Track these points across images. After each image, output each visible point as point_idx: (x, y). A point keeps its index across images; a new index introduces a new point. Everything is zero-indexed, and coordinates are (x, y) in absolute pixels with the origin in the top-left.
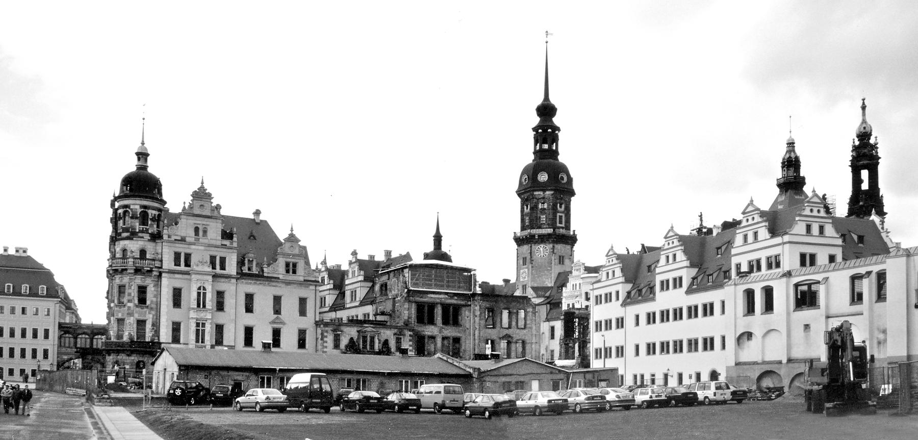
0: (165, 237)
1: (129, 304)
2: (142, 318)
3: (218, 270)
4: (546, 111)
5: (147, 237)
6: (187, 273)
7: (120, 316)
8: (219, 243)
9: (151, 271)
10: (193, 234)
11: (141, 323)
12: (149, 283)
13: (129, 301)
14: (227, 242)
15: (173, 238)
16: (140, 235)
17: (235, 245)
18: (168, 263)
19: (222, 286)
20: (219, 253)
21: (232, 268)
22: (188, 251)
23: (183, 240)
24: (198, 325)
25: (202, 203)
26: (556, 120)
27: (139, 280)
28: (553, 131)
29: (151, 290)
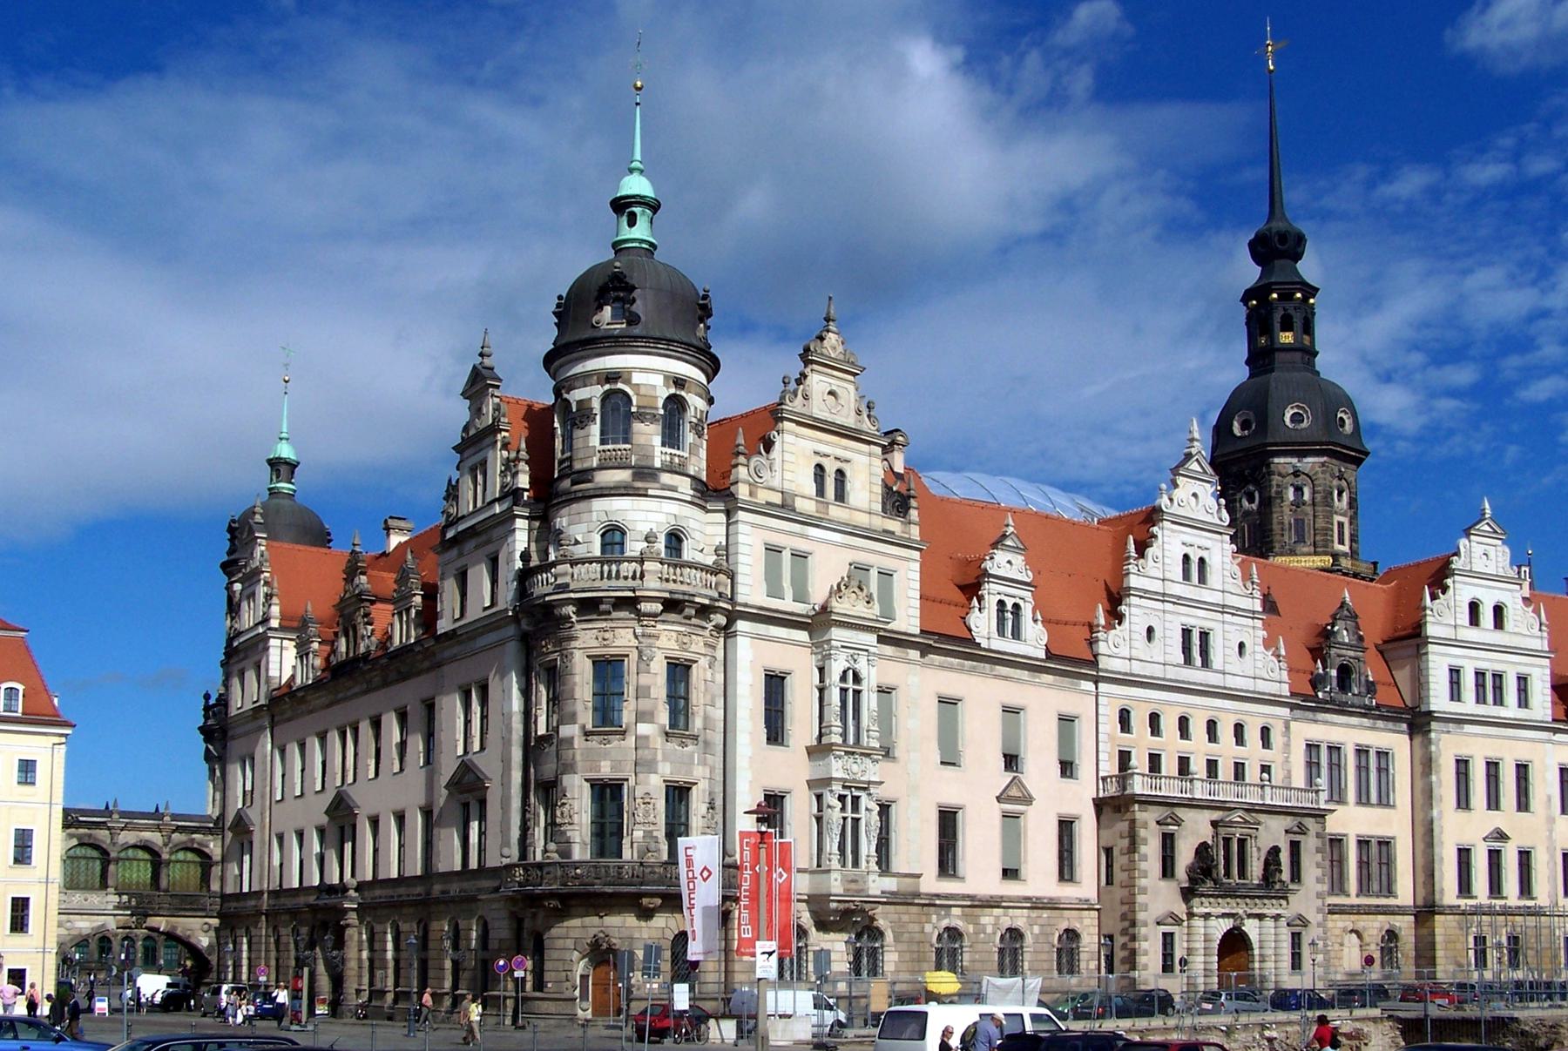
1: (644, 729)
2: (681, 778)
5: (685, 486)
7: (606, 771)
9: (704, 611)
10: (810, 488)
12: (697, 645)
13: (641, 717)
14: (894, 525)
16: (666, 478)
17: (915, 532)
18: (752, 591)
22: (802, 545)
23: (785, 509)
25: (835, 384)
27: (669, 638)
28: (1305, 299)
29: (703, 677)
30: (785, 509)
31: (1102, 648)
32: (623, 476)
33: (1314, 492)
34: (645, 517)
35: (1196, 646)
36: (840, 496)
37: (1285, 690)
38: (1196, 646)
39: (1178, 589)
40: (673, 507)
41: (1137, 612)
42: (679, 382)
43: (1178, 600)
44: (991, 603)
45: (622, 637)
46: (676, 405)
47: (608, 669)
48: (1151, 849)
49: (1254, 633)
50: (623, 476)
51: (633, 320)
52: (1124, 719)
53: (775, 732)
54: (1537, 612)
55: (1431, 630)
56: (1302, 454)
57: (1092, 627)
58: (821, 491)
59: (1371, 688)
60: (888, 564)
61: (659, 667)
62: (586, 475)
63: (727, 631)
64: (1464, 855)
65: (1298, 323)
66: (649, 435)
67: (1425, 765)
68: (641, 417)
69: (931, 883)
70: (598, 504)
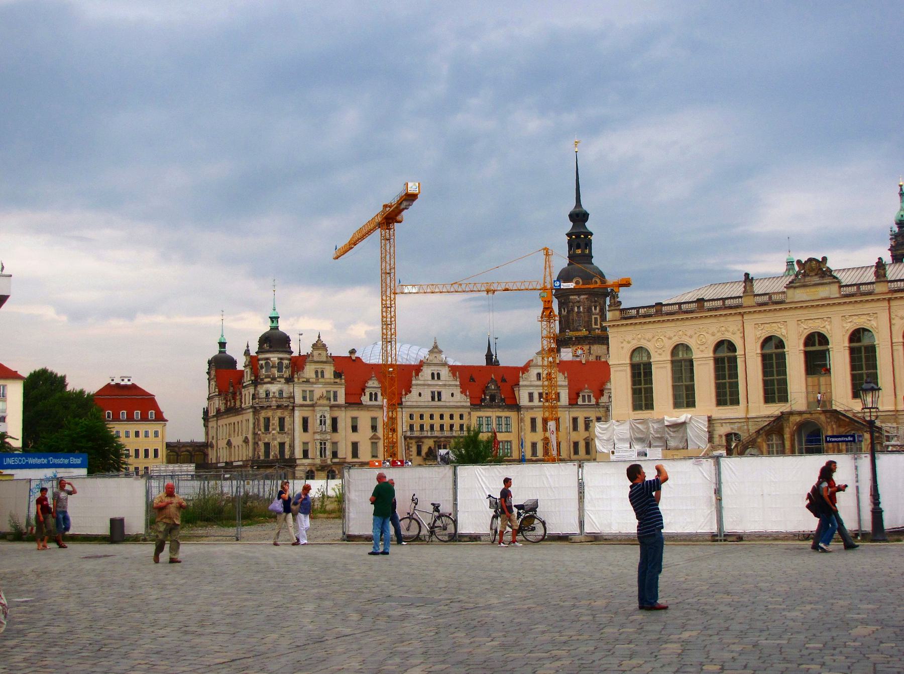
0: (296, 380)
3: (332, 402)
4: (579, 217)
5: (283, 380)
6: (313, 406)
7: (266, 440)
8: (332, 381)
11: (282, 445)
12: (286, 414)
13: (274, 429)
14: (338, 380)
15: (301, 380)
18: (298, 400)
19: (336, 413)
20: (332, 389)
21: (341, 400)
23: (308, 381)
24: (321, 444)
26: (588, 225)
27: (279, 413)
28: (586, 236)
29: (288, 420)
30: (308, 381)
31: (403, 400)
32: (269, 380)
33: (584, 308)
34: (274, 388)
35: (437, 396)
36: (323, 376)
37: (469, 404)
38: (437, 396)
39: (429, 382)
40: (280, 386)
41: (415, 391)
42: (281, 359)
43: (429, 385)
44: (368, 394)
45: (270, 414)
46: (280, 364)
47: (267, 420)
48: (414, 449)
49: (457, 391)
50: (269, 380)
51: (271, 347)
52: (411, 417)
53: (305, 429)
54: (564, 374)
55: (521, 383)
56: (579, 295)
57: (401, 394)
58: (317, 376)
59: (503, 400)
60: (335, 390)
61: (277, 419)
62: (262, 380)
63: (293, 410)
64: (534, 445)
65: (583, 245)
66: (275, 371)
67: (521, 420)
68: (273, 367)
69: (349, 459)
70: (265, 386)
